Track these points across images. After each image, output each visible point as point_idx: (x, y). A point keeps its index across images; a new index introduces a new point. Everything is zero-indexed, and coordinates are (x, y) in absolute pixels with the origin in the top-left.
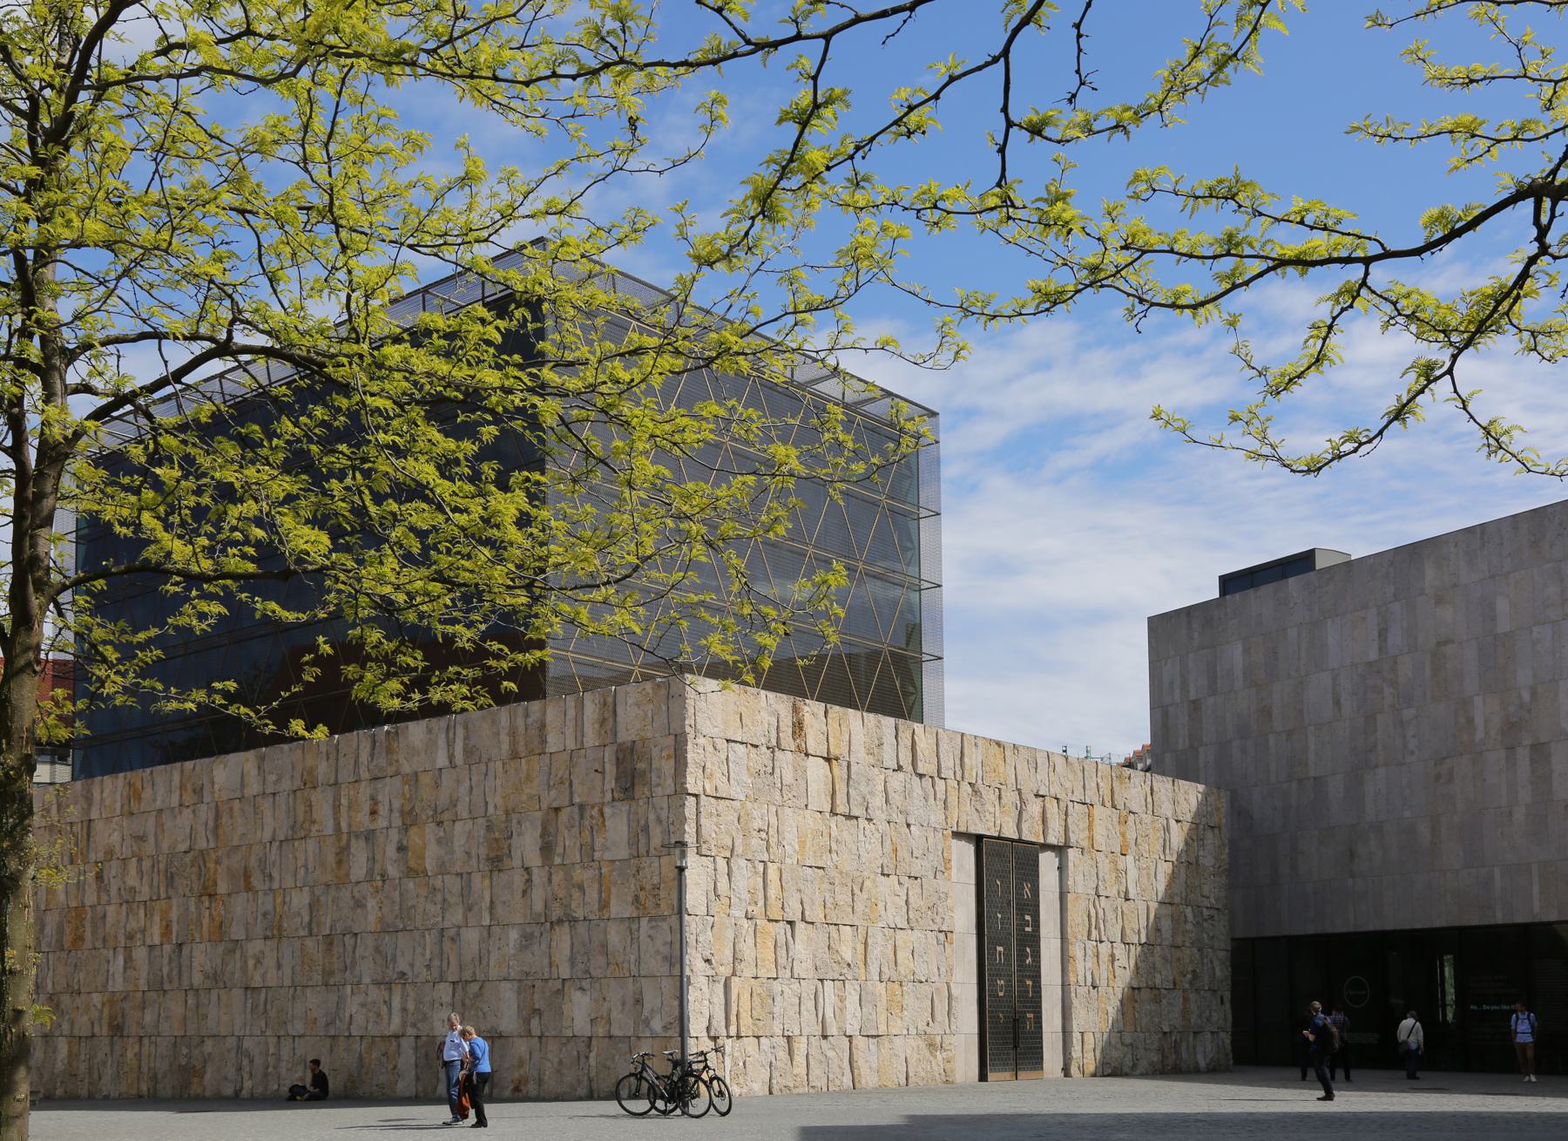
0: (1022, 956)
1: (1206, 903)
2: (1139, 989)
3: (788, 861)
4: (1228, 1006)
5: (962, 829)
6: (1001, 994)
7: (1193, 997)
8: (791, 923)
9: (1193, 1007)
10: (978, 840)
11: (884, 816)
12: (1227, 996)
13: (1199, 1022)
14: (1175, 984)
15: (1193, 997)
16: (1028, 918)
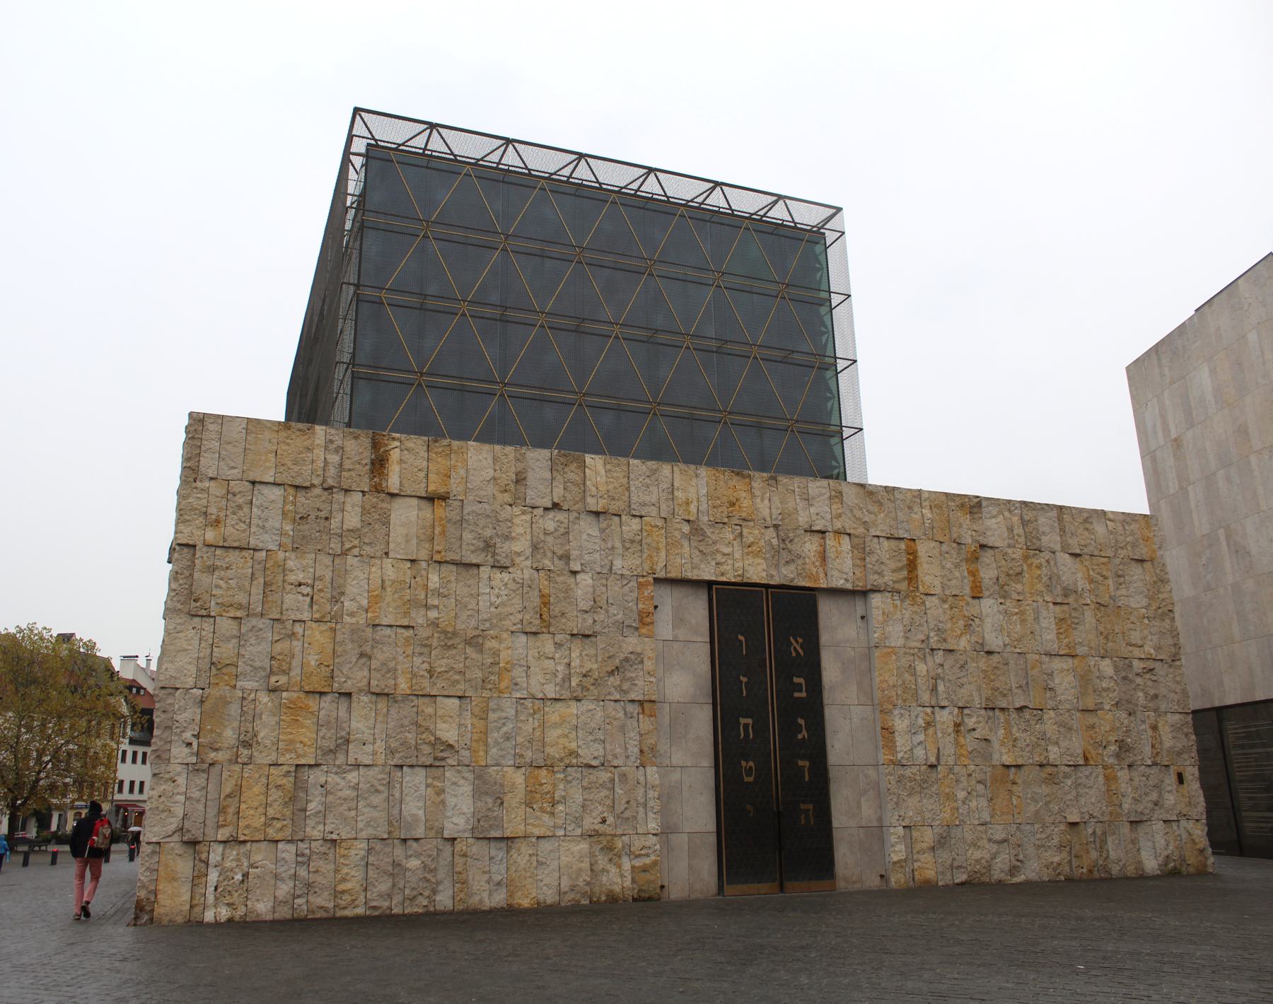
0: (788, 728)
1: (1137, 652)
2: (1018, 766)
3: (347, 619)
4: (1194, 786)
5: (673, 574)
6: (747, 779)
7: (1123, 775)
8: (349, 695)
9: (1123, 787)
10: (709, 584)
11: (528, 563)
12: (1192, 772)
13: (1140, 808)
14: (1086, 759)
15: (1123, 775)
16: (796, 680)
